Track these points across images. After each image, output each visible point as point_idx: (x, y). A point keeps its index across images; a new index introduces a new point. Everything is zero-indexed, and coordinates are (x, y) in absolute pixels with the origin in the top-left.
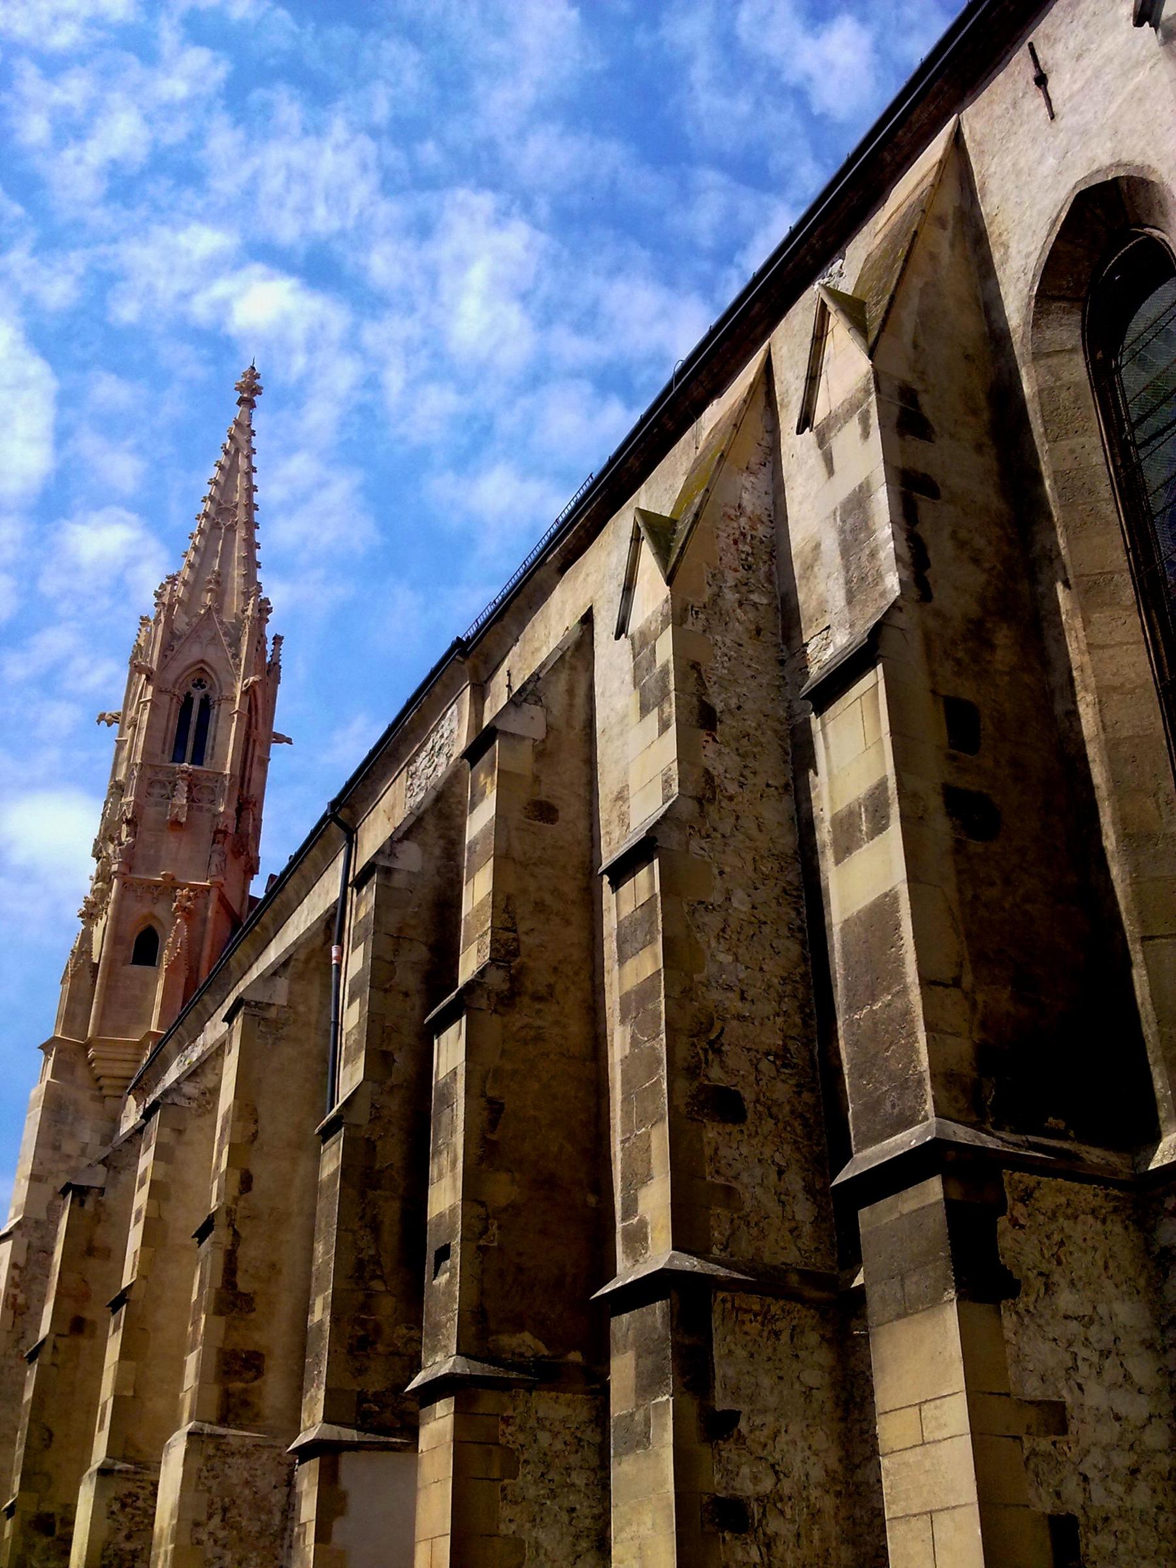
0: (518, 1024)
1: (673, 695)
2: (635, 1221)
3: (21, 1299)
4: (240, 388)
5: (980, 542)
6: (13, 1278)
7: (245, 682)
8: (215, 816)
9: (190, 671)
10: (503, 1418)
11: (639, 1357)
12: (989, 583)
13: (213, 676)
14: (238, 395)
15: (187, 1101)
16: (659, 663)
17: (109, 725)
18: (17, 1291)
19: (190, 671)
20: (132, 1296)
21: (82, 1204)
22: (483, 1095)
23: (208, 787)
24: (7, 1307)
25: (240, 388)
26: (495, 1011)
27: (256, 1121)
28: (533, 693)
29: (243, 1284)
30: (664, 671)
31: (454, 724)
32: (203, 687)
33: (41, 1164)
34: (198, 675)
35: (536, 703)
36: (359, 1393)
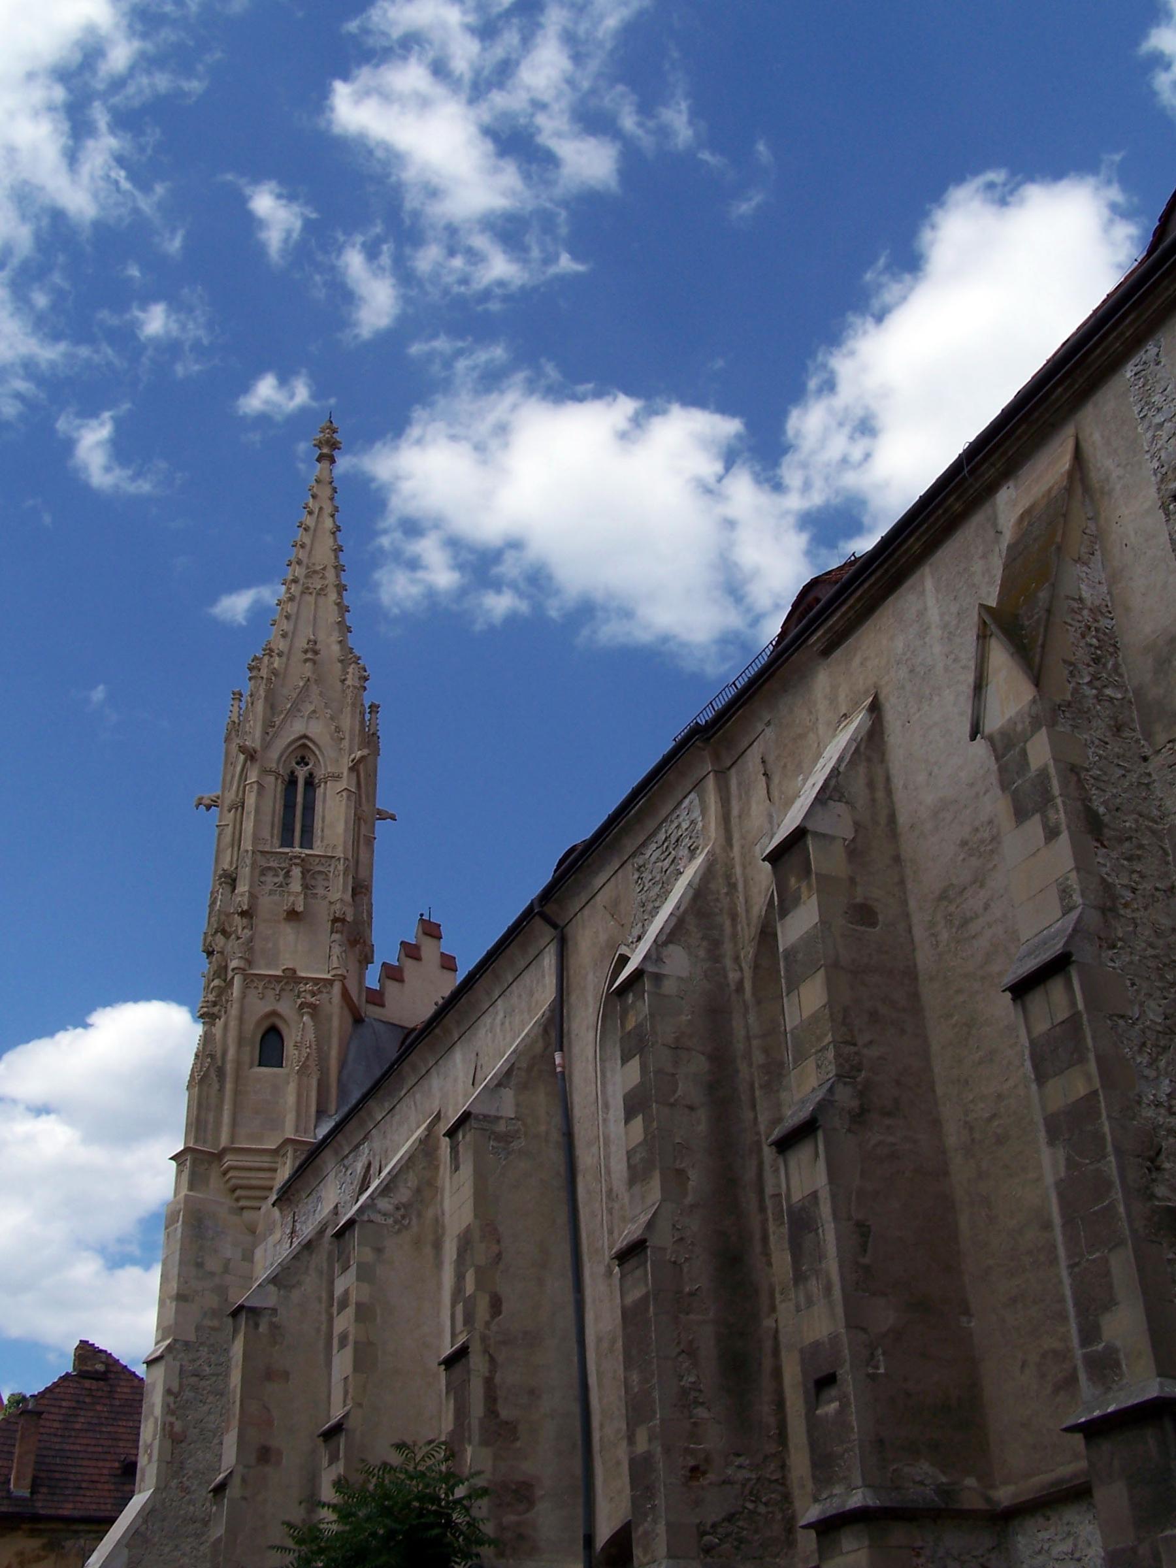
1: (1059, 801)
2: (1100, 1347)
3: (178, 1427)
6: (168, 1406)
7: (353, 756)
8: (331, 903)
10: (914, 1549)
13: (317, 752)
15: (383, 1218)
17: (208, 807)
18: (173, 1419)
20: (349, 1424)
21: (257, 1325)
22: (850, 1219)
23: (320, 872)
24: (164, 1436)
25: (319, 446)
26: (849, 1130)
27: (498, 1241)
28: (835, 789)
29: (505, 1413)
31: (696, 814)
32: (307, 764)
33: (186, 1283)
34: (299, 754)
35: (839, 801)
36: (698, 1525)
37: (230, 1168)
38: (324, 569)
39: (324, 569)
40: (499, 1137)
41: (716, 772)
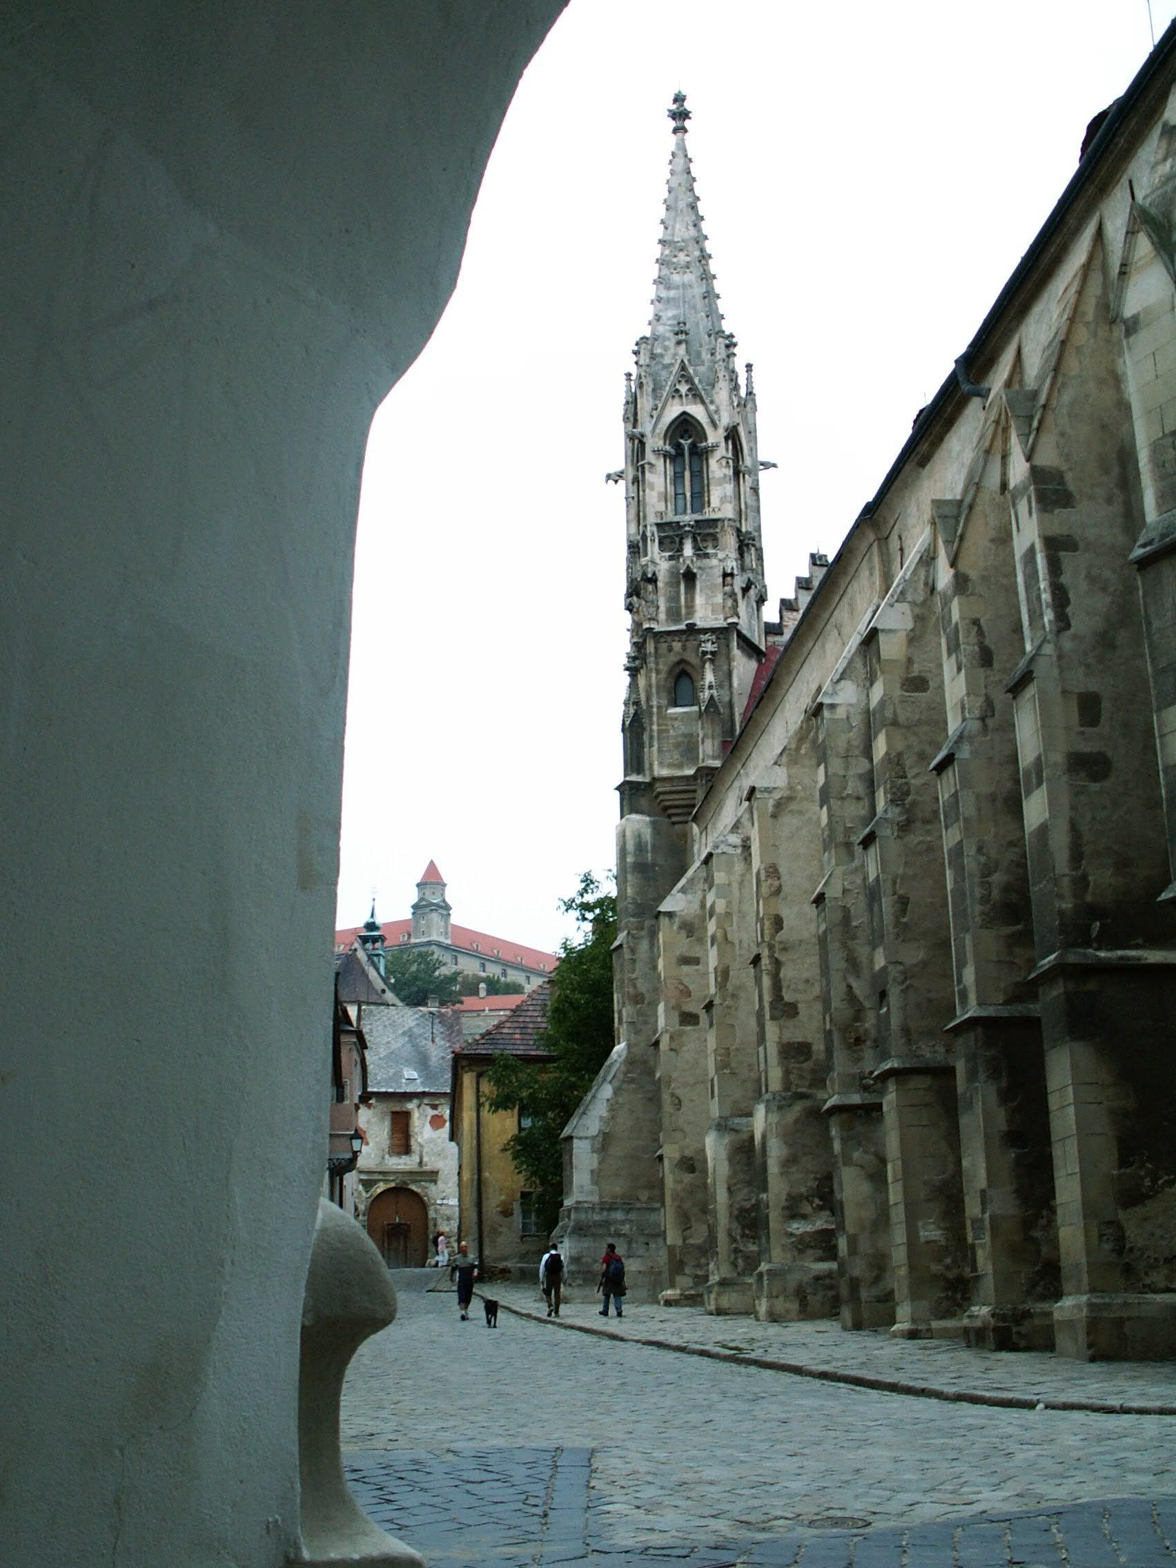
0: (916, 841)
5: (1107, 574)
11: (967, 1061)
12: (1112, 602)
14: (673, 124)
16: (954, 621)
17: (616, 482)
27: (779, 878)
29: (788, 997)
30: (957, 624)
37: (659, 794)
41: (879, 539)
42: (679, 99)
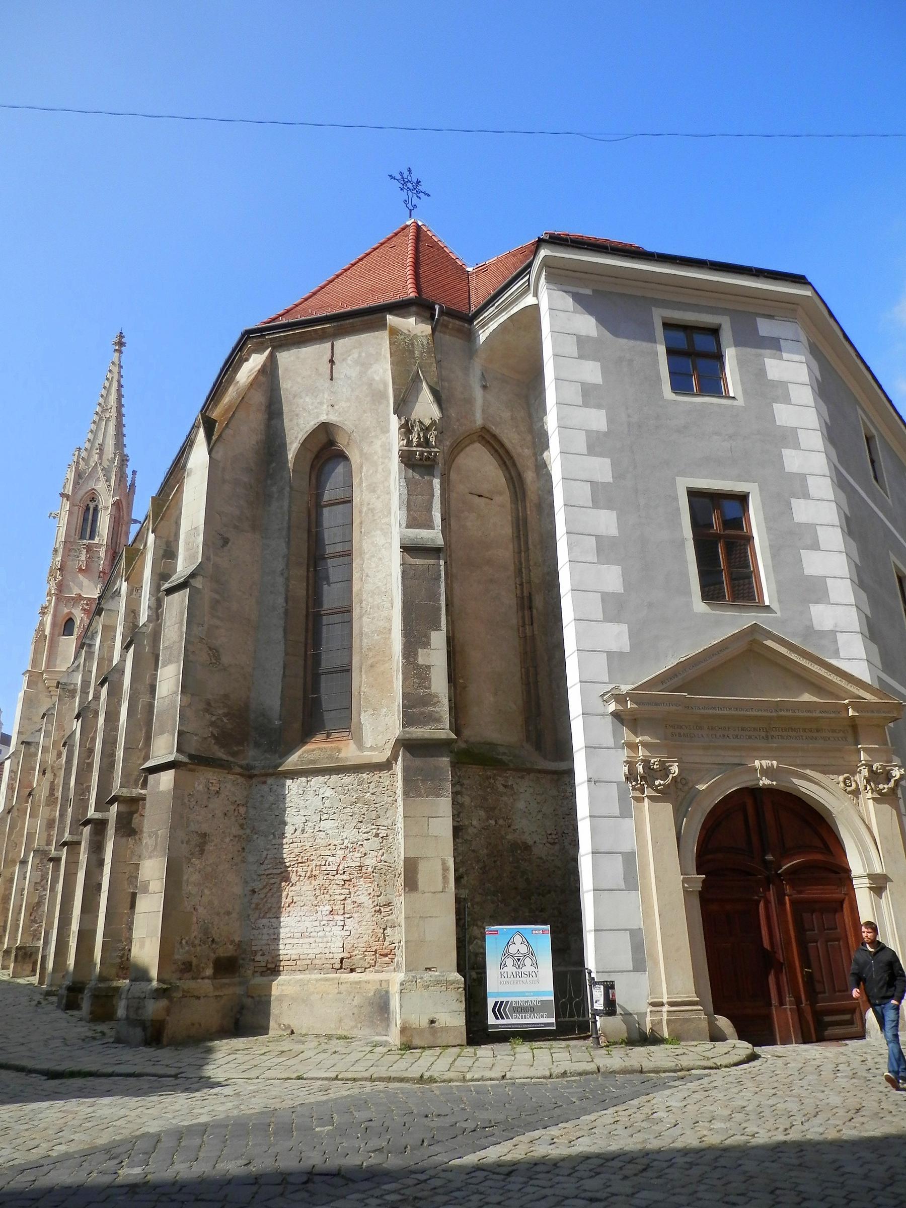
4: (115, 344)
9: (88, 494)
19: (88, 494)
32: (95, 501)
38: (111, 408)
39: (111, 408)
40: (69, 691)
42: (121, 336)
